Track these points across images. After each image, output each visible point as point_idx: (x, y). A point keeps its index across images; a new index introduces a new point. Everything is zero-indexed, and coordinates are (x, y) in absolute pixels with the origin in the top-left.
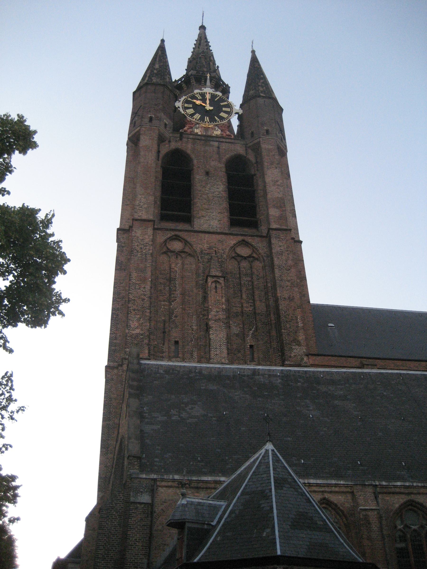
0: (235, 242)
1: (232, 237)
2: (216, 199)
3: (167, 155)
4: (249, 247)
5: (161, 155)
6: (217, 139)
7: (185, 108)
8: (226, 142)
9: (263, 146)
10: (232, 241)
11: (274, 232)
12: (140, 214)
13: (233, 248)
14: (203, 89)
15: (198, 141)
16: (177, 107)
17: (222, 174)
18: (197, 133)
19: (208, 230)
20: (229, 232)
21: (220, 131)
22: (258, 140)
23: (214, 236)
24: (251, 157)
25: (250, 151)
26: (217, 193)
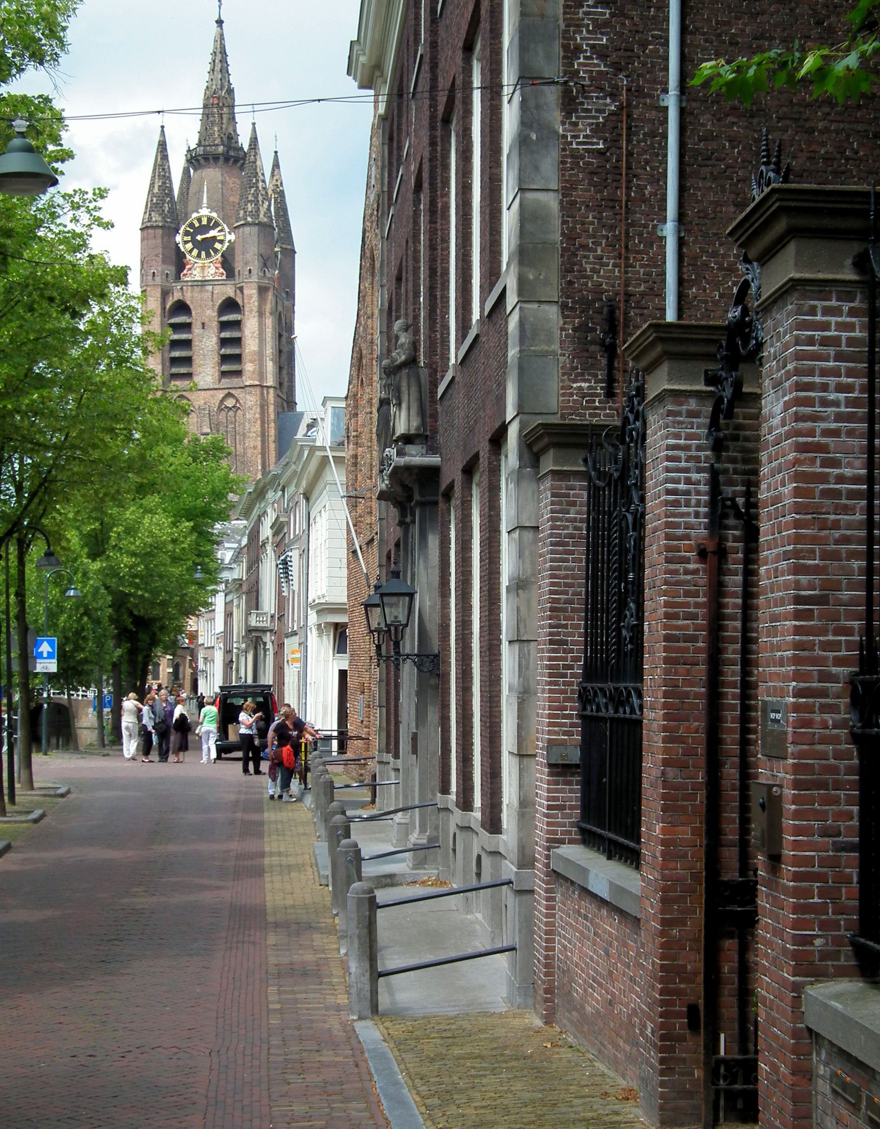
0: (221, 396)
3: (172, 305)
7: (186, 242)
10: (221, 395)
13: (222, 401)
24: (240, 302)
25: (238, 291)
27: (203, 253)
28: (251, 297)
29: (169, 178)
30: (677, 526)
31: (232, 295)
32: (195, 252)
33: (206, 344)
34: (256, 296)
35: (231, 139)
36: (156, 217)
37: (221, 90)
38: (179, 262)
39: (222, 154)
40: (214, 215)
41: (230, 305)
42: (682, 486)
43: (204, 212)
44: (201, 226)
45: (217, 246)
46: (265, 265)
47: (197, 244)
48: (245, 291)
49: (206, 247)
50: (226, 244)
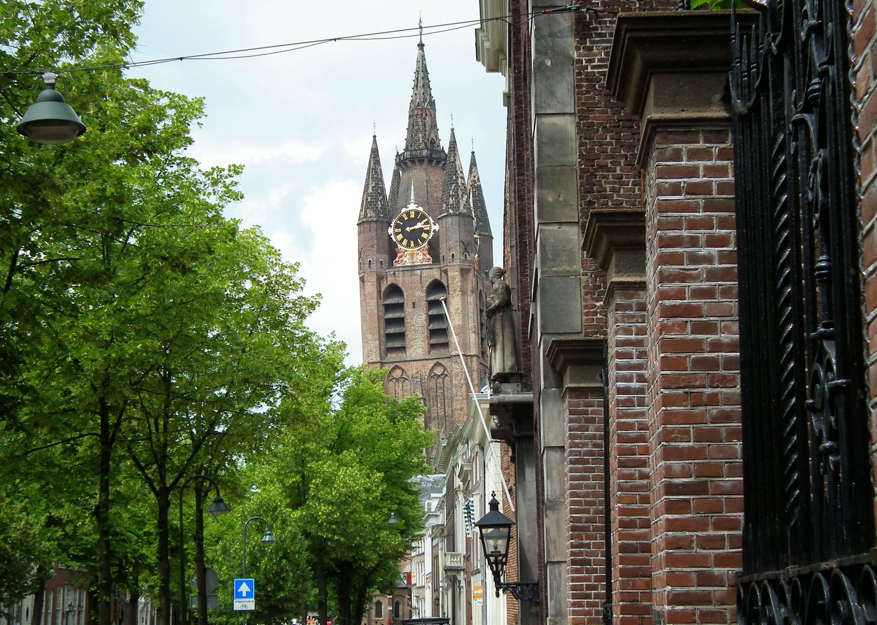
0: (431, 365)
3: (386, 289)
7: (397, 234)
10: (431, 364)
25: (443, 274)
27: (412, 243)
28: (454, 278)
29: (381, 180)
30: (630, 426)
31: (438, 277)
32: (405, 242)
33: (417, 321)
35: (433, 143)
36: (371, 213)
37: (424, 102)
38: (392, 251)
39: (426, 157)
40: (421, 209)
41: (437, 286)
42: (634, 384)
43: (412, 207)
44: (410, 219)
45: (424, 235)
46: (466, 250)
47: (406, 235)
48: (450, 274)
49: (414, 237)
50: (432, 234)
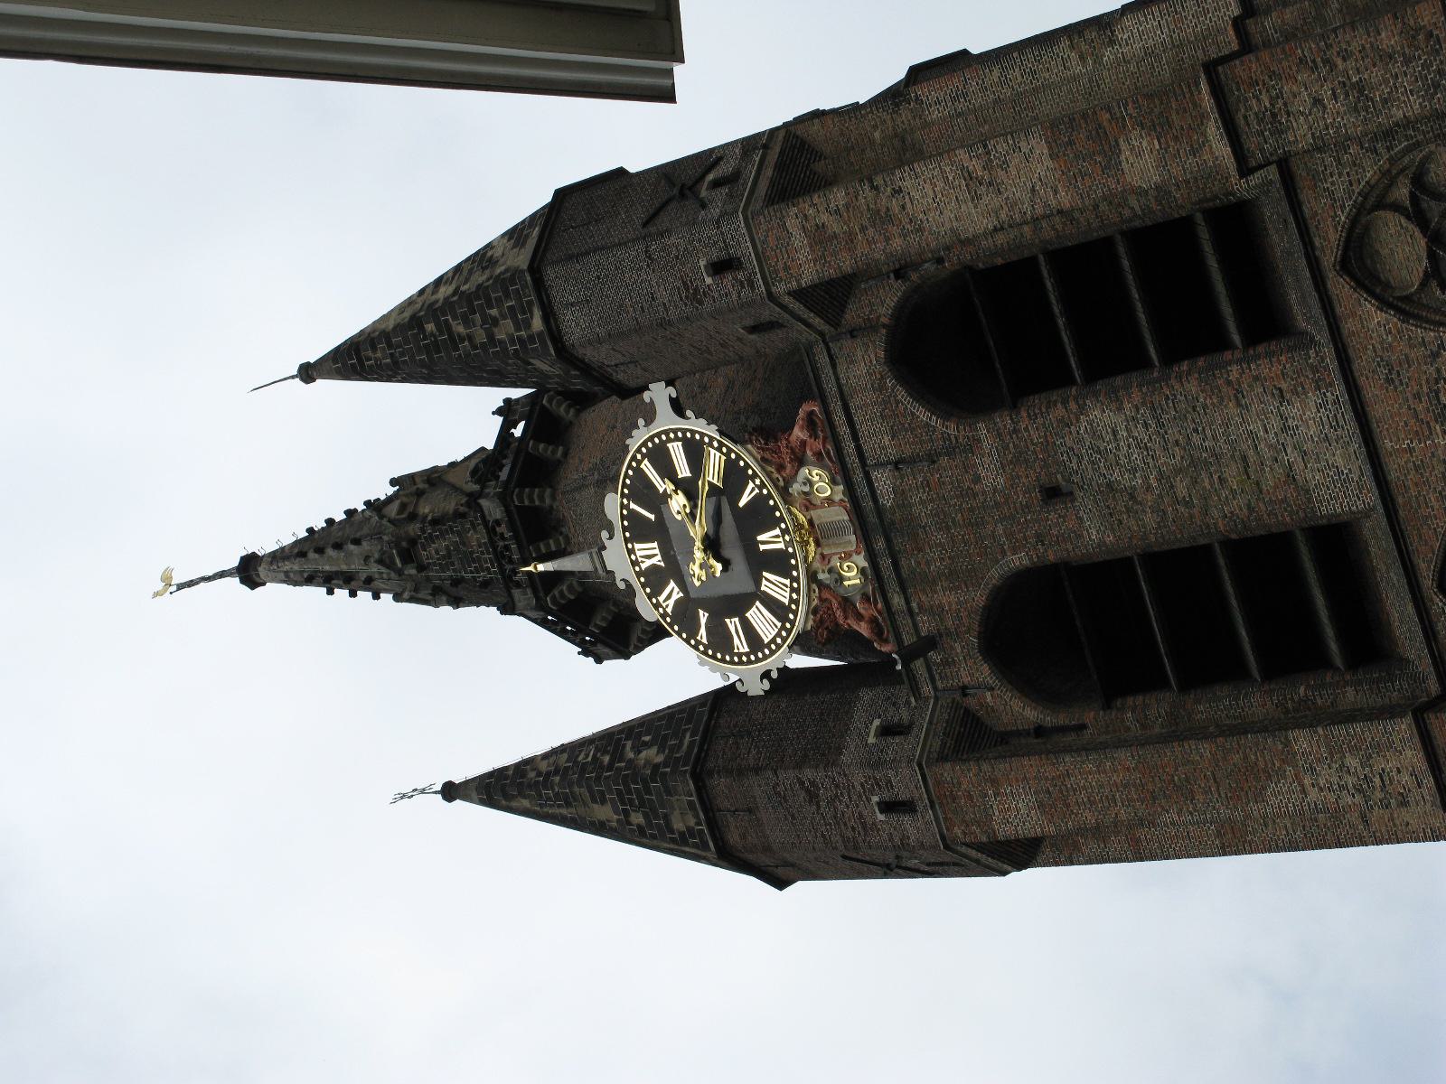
0: (1369, 307)
1: (1349, 326)
2: (1173, 433)
3: (1028, 686)
4: (1367, 228)
5: (1049, 720)
6: (858, 476)
8: (855, 437)
9: (809, 274)
10: (1369, 322)
11: (1251, 143)
12: (1405, 778)
13: (1405, 307)
14: (622, 586)
15: (903, 562)
16: (766, 685)
17: (1033, 424)
18: (862, 571)
19: (1356, 445)
20: (1323, 337)
21: (805, 471)
22: (787, 300)
23: (1376, 411)
24: (884, 301)
25: (853, 315)
26: (1139, 432)
33: (1143, 458)
34: (805, 205)
